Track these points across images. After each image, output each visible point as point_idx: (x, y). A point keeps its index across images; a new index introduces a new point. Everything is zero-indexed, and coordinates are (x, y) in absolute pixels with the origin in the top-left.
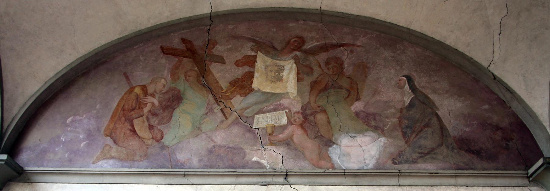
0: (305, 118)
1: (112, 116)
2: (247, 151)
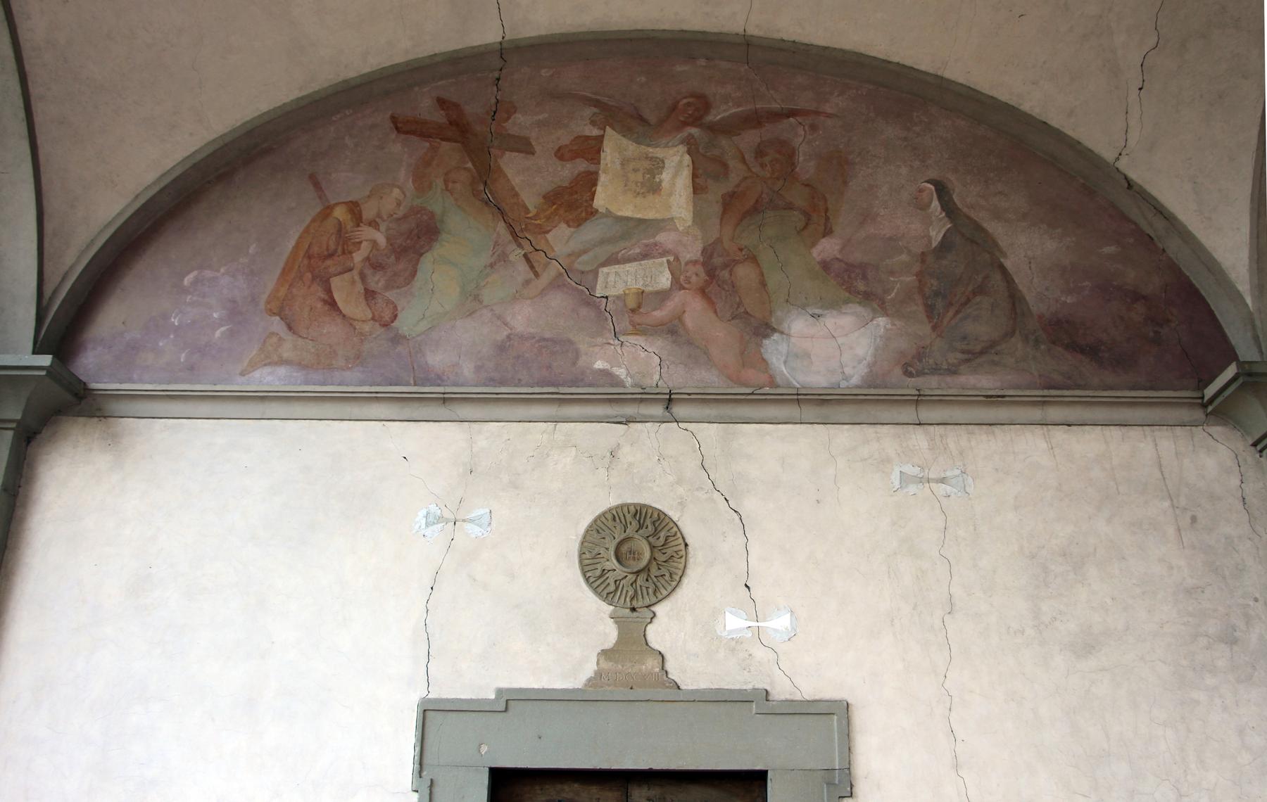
0: (711, 273)
1: (284, 269)
2: (583, 347)
